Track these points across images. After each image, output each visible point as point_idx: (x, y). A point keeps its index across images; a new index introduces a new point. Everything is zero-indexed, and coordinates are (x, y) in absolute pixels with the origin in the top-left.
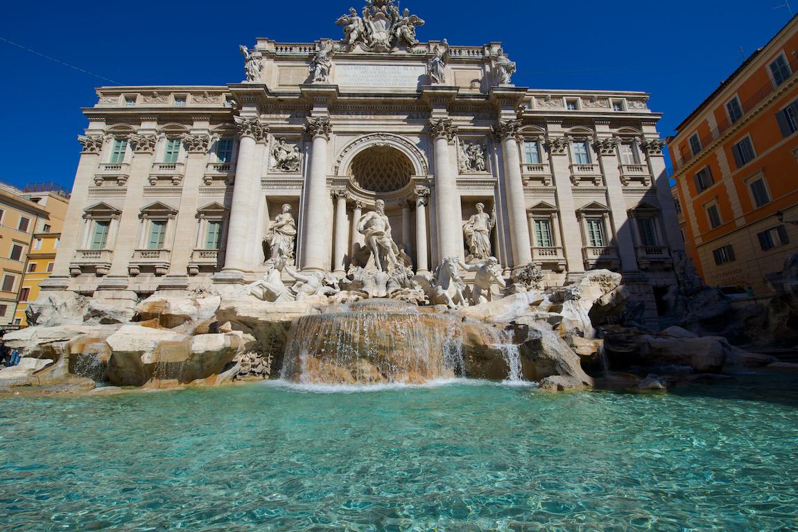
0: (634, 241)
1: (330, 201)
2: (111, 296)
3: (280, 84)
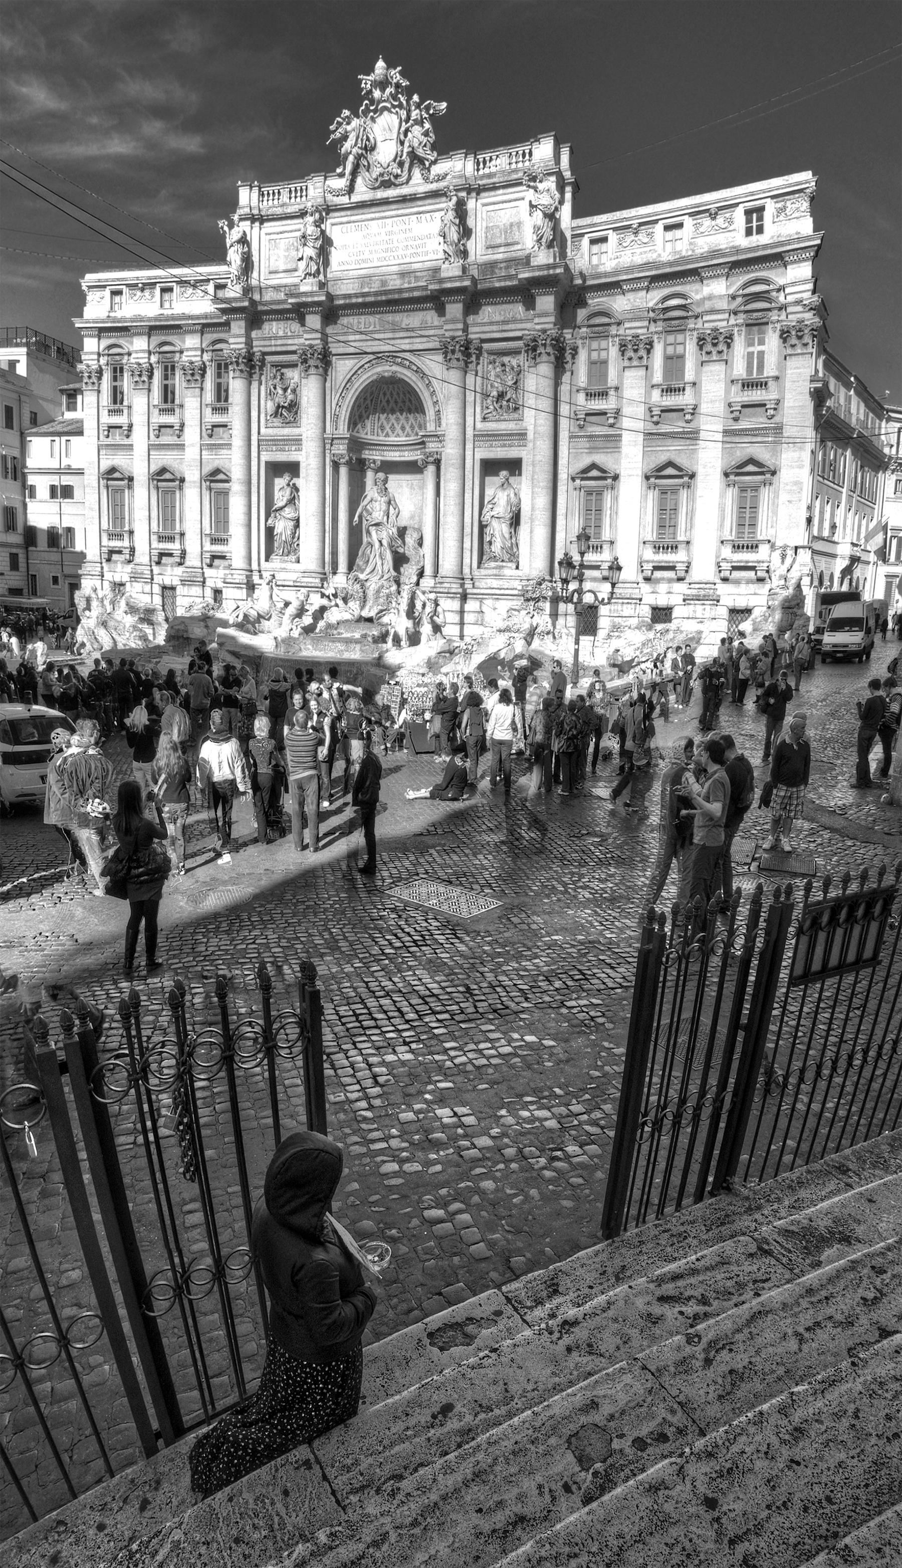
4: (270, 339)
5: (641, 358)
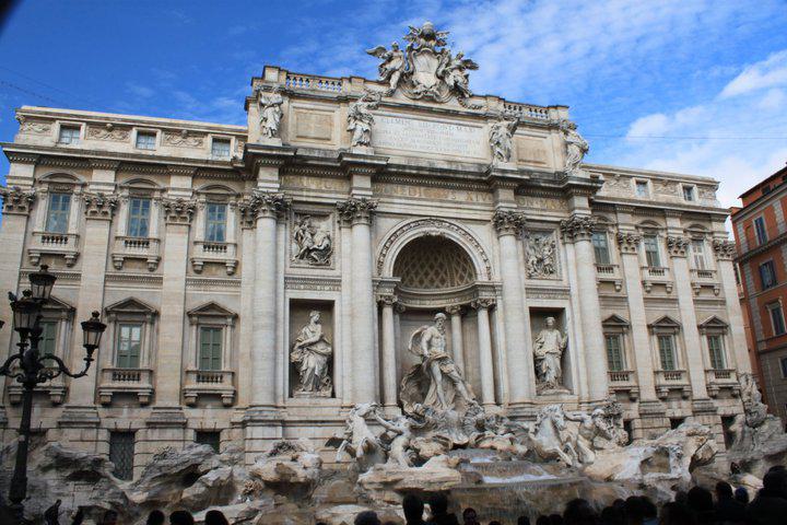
0: (704, 363)
1: (376, 309)
2: (78, 437)
3: (300, 134)
4: (302, 190)
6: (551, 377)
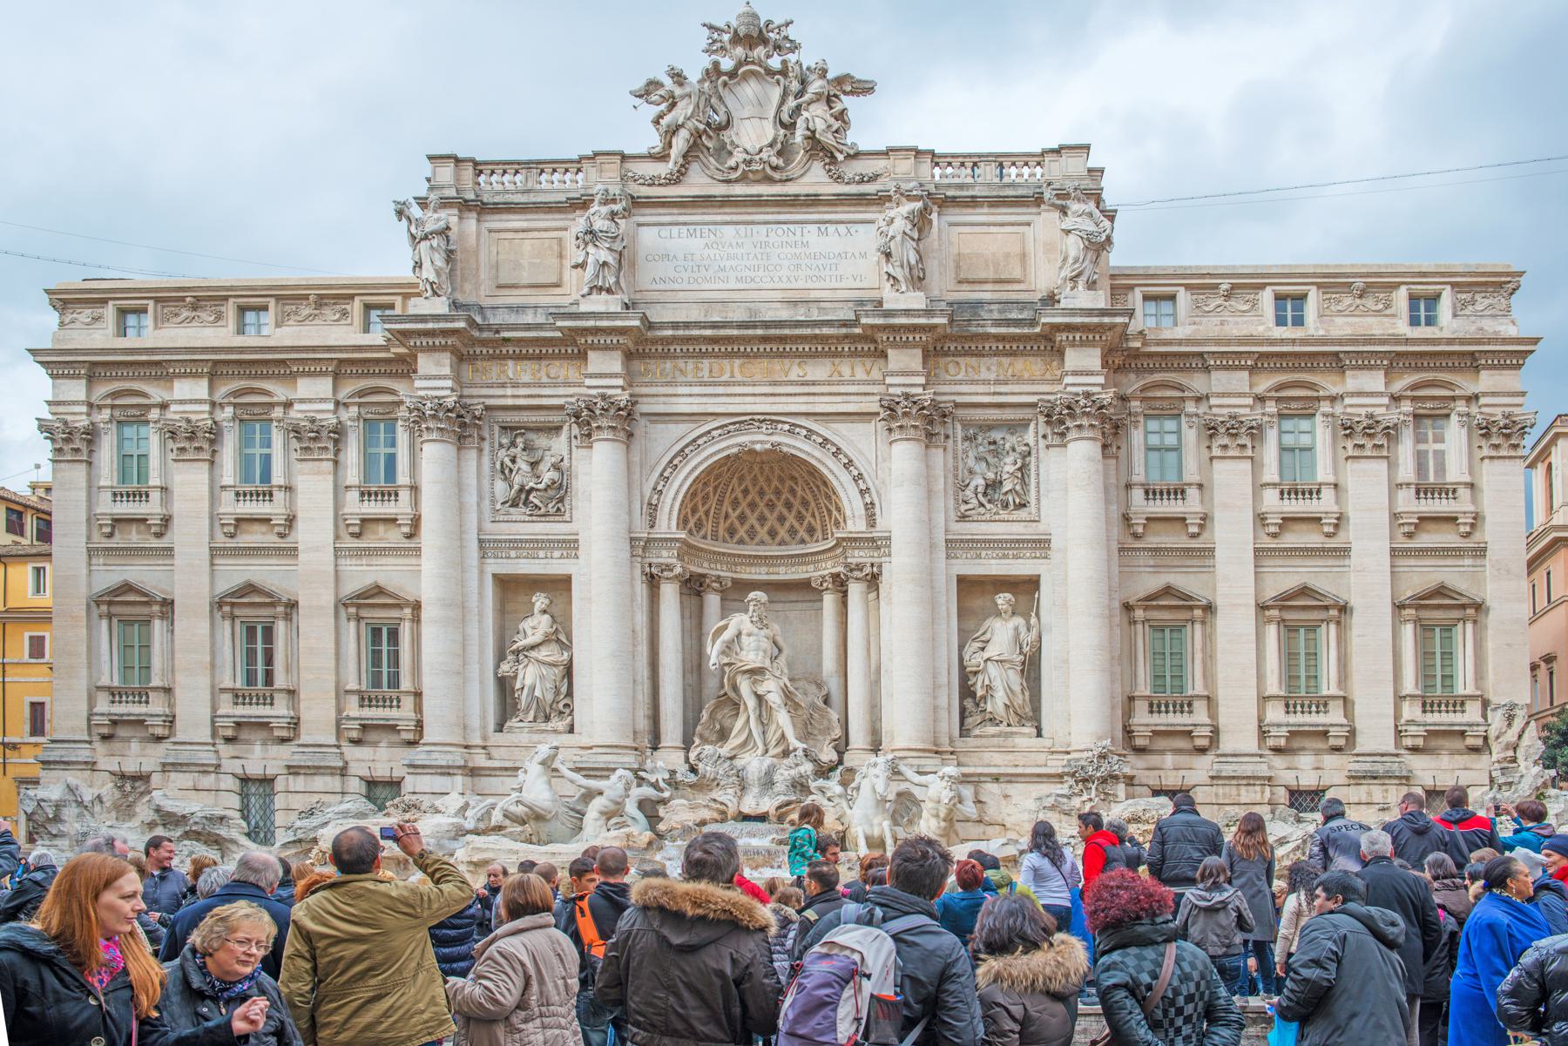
1: (641, 589)
5: (1243, 446)
6: (997, 704)
